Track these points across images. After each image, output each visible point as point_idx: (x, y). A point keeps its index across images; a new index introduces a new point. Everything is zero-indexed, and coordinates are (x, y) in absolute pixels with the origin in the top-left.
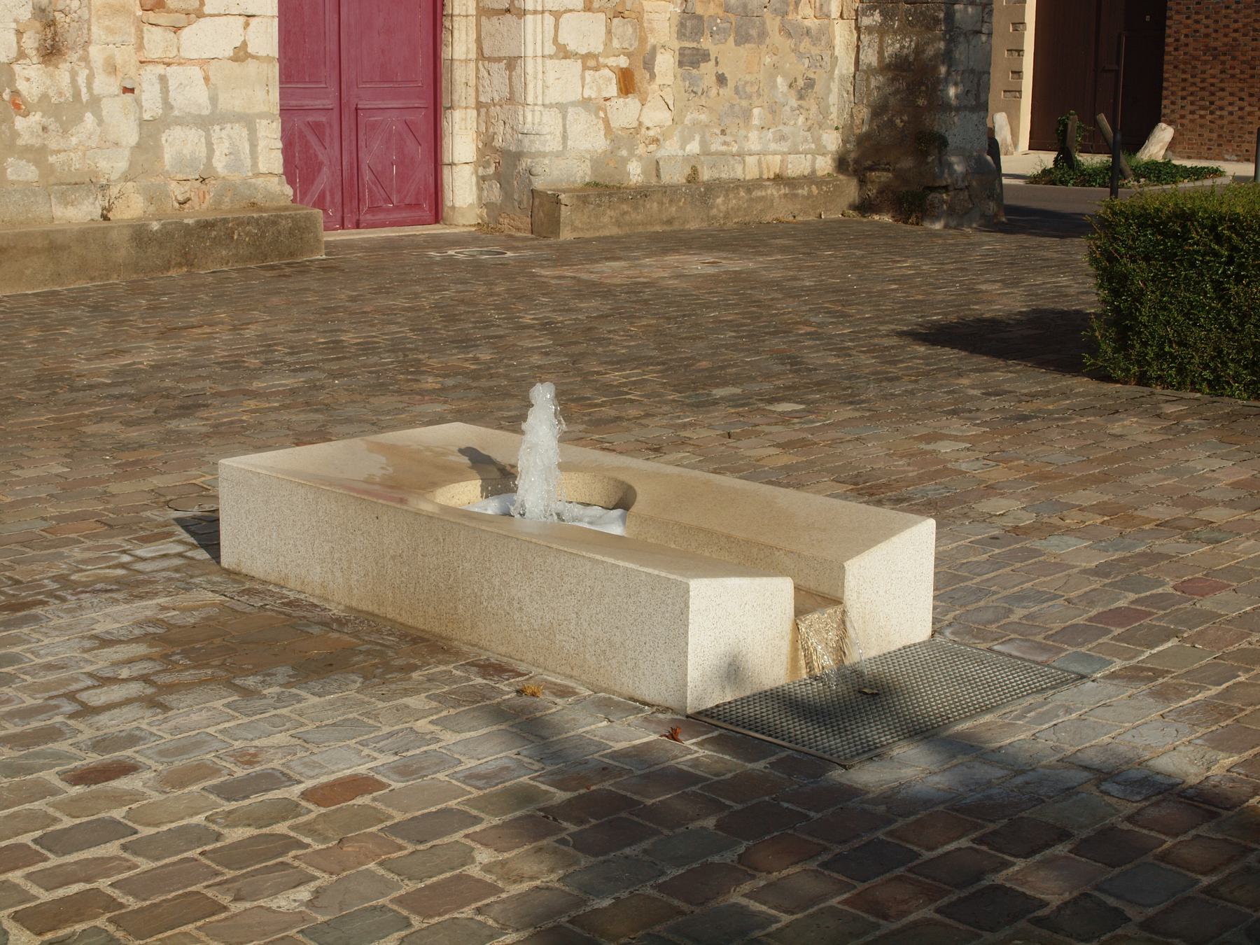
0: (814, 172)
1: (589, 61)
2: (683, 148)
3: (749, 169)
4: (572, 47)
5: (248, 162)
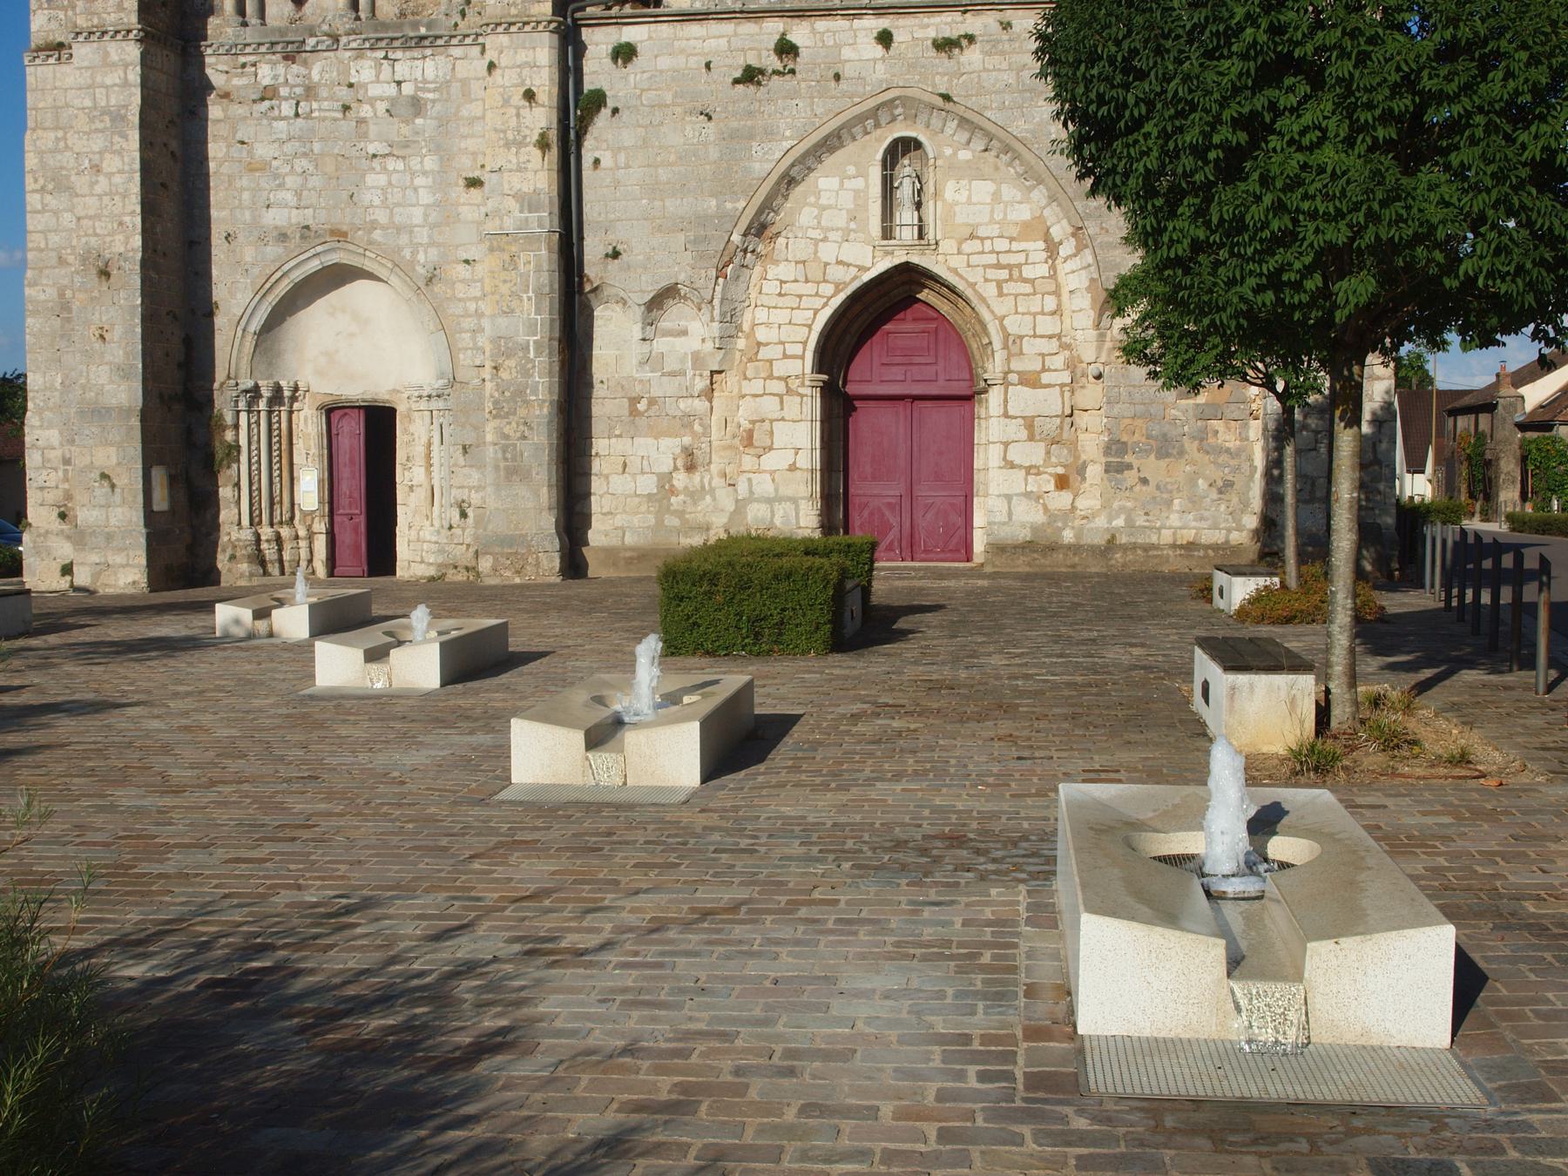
0: (1175, 540)
2: (1110, 522)
3: (1166, 537)
4: (1017, 462)
5: (794, 521)
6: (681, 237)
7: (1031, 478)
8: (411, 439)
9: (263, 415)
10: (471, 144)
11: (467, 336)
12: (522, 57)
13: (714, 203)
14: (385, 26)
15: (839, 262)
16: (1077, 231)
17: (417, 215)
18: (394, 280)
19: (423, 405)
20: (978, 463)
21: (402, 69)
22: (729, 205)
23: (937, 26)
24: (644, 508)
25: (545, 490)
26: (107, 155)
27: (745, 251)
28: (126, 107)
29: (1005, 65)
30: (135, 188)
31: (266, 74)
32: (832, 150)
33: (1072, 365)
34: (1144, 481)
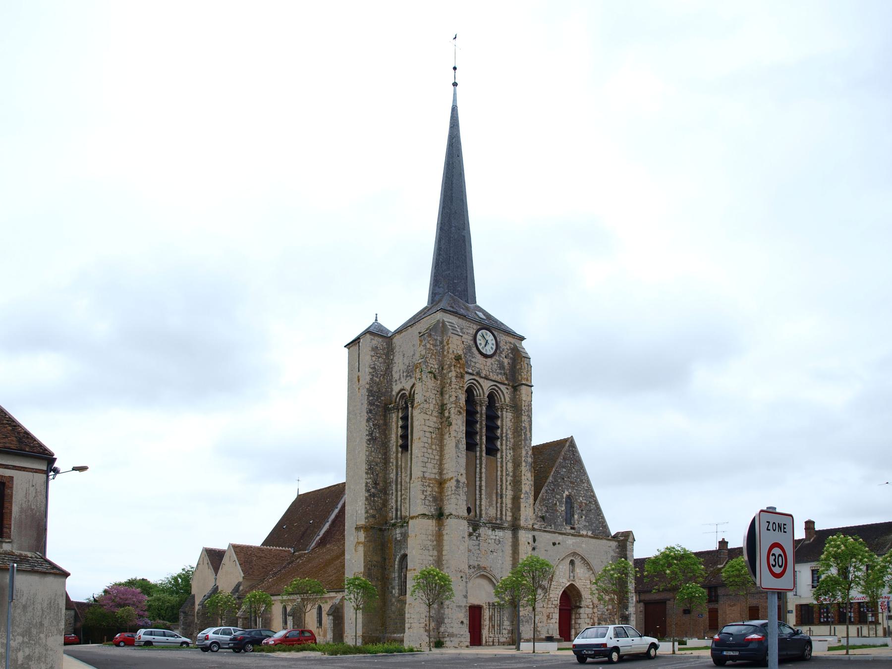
8: (486, 614)
12: (527, 535)
33: (593, 604)
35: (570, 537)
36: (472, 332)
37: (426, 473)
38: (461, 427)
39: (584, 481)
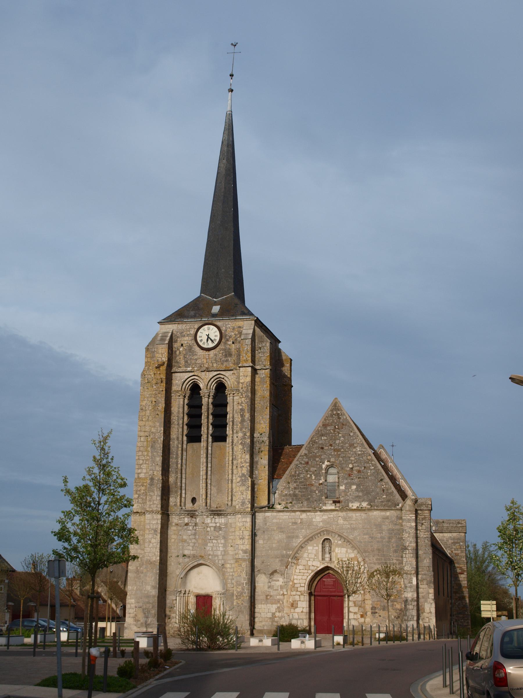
1: (355, 613)
6: (278, 559)
7: (355, 615)
9: (182, 597)
10: (232, 537)
11: (230, 580)
12: (244, 520)
13: (285, 552)
14: (213, 511)
15: (313, 566)
16: (364, 560)
17: (219, 553)
18: (214, 567)
19: (219, 596)
20: (344, 612)
21: (217, 520)
22: (288, 553)
23: (333, 514)
24: (269, 621)
25: (247, 616)
26: (152, 539)
27: (292, 563)
28: (157, 528)
29: (348, 523)
30: (158, 546)
31: (186, 520)
32: (311, 541)
34: (380, 616)
35: (319, 513)
36: (193, 332)
37: (142, 474)
38: (159, 429)
39: (355, 445)
